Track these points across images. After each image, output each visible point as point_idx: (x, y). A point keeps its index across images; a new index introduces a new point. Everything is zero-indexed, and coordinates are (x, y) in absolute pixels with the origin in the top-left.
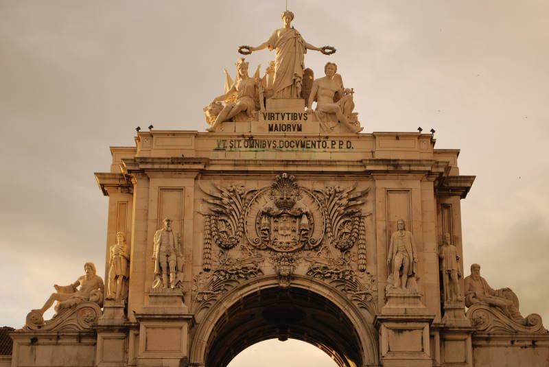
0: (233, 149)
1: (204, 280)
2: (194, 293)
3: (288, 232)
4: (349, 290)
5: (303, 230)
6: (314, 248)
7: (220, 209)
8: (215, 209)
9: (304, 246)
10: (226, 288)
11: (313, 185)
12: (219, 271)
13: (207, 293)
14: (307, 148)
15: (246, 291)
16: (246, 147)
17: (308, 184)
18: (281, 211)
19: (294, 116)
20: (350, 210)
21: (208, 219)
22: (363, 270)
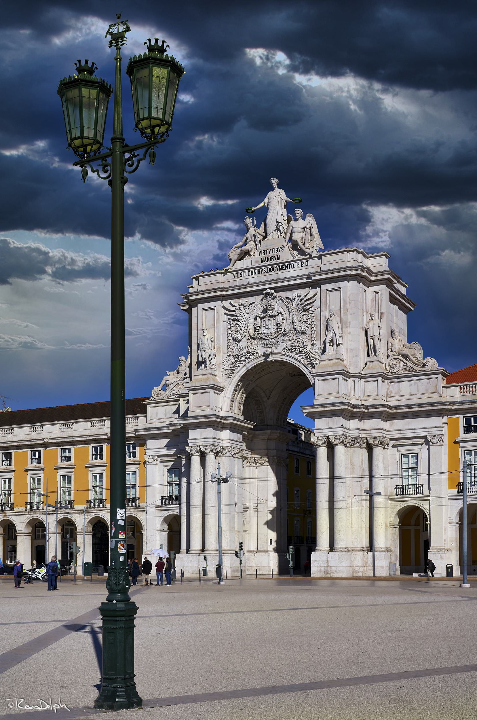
0: (242, 278)
3: (270, 327)
4: (305, 358)
5: (278, 324)
6: (286, 334)
7: (234, 318)
10: (240, 365)
12: (235, 355)
13: (230, 369)
14: (283, 270)
15: (251, 365)
16: (249, 275)
17: (283, 294)
18: (266, 314)
19: (276, 250)
20: (305, 308)
21: (229, 324)
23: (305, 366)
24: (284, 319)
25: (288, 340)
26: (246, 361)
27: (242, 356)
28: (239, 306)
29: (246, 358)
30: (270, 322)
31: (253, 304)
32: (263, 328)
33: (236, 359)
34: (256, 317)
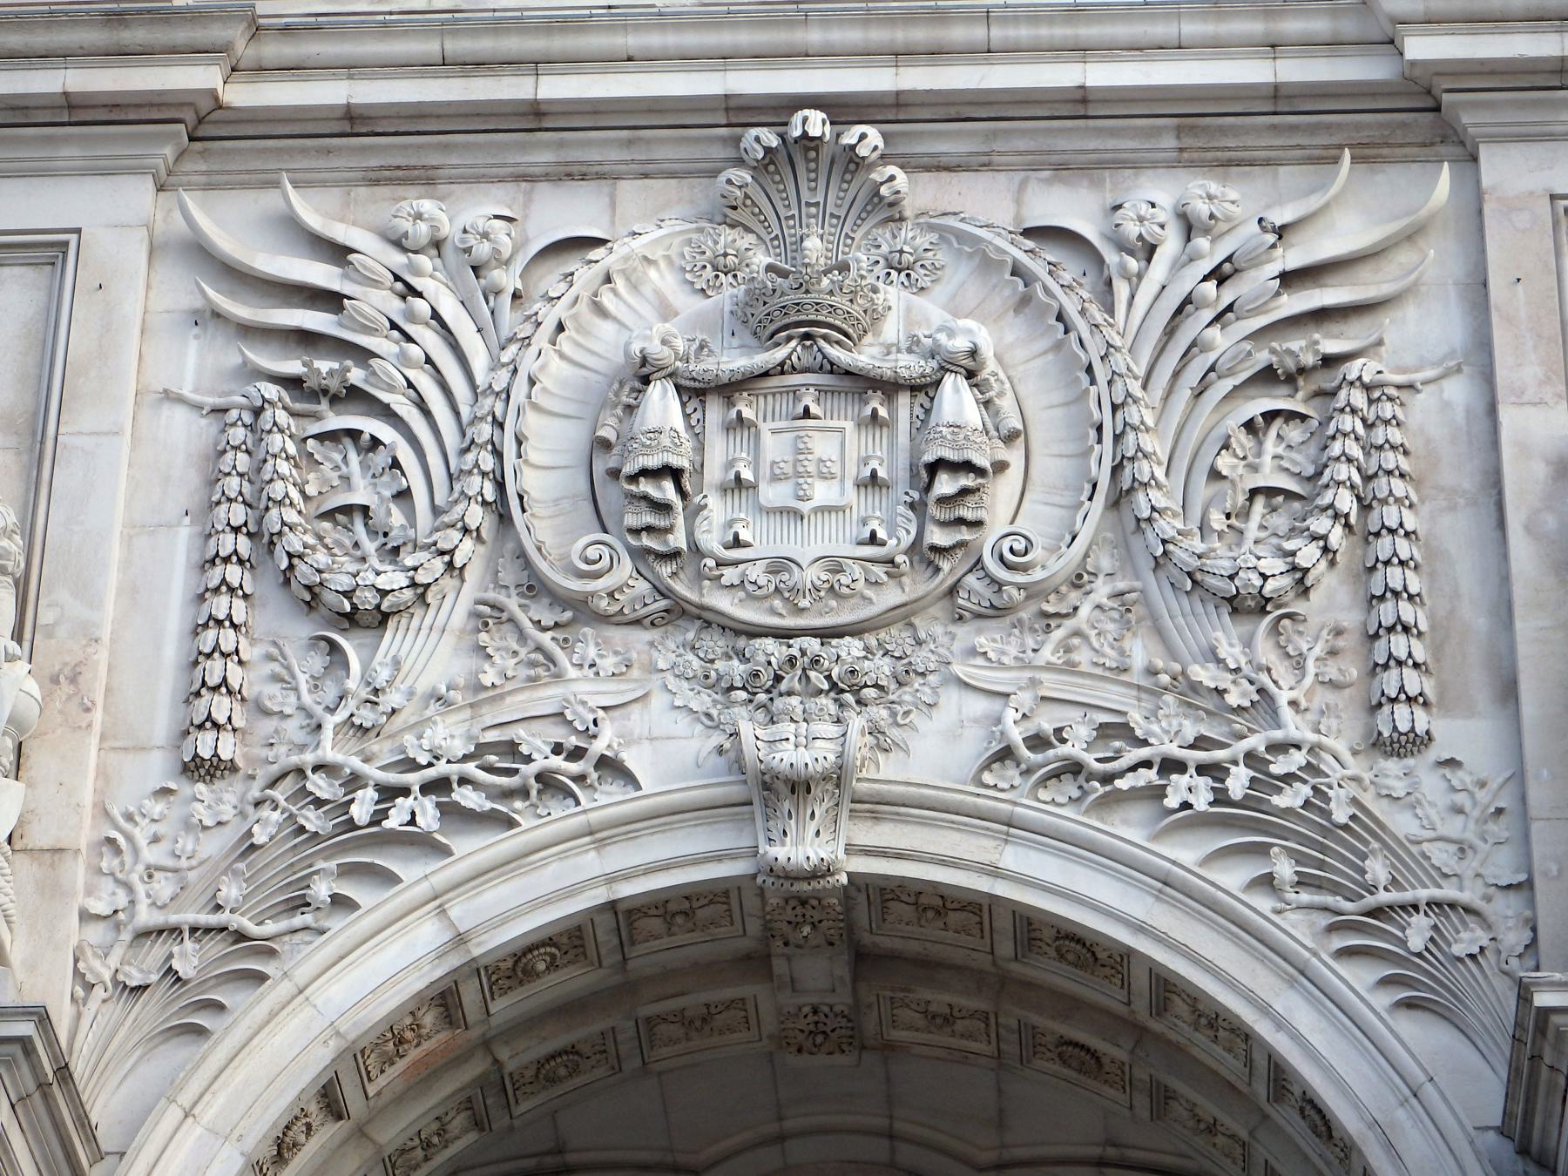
1: (187, 843)
2: (96, 934)
4: (1302, 882)
5: (935, 467)
7: (324, 366)
8: (293, 367)
9: (953, 591)
10: (348, 889)
11: (1018, 202)
12: (300, 772)
18: (780, 354)
20: (1296, 344)
21: (238, 435)
22: (1409, 744)
23: (1300, 973)
24: (1010, 438)
25: (1049, 667)
26: (445, 851)
27: (405, 791)
28: (397, 259)
29: (453, 814)
30: (823, 446)
31: (597, 253)
32: (717, 509)
33: (312, 820)
34: (644, 374)
